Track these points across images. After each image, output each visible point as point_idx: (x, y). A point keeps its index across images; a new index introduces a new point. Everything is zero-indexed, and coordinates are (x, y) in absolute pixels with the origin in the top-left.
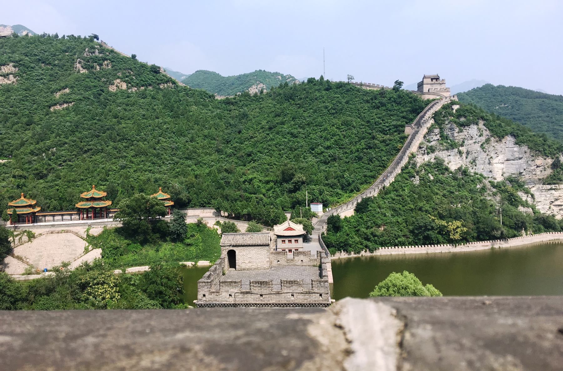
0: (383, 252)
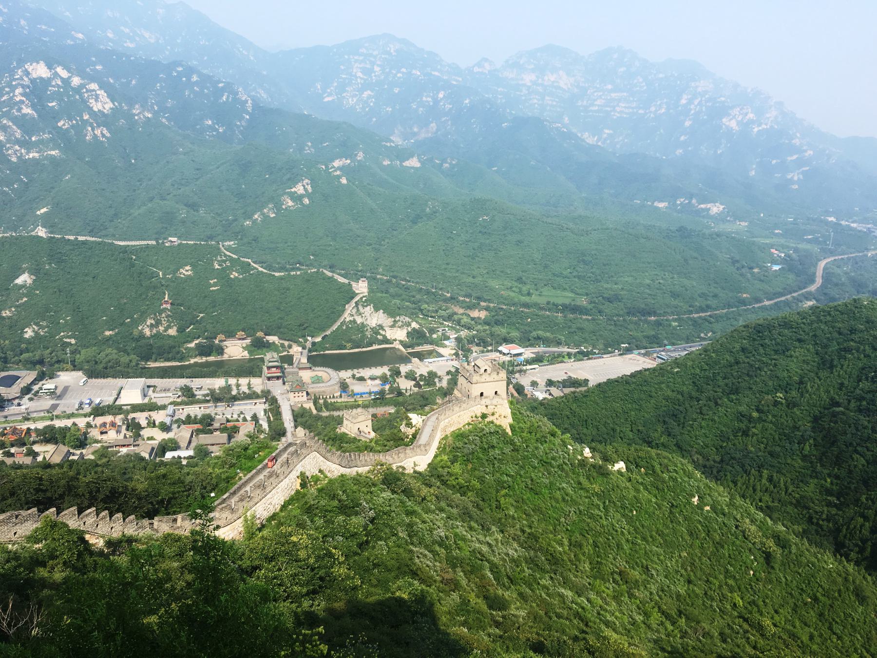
0: (327, 352)
